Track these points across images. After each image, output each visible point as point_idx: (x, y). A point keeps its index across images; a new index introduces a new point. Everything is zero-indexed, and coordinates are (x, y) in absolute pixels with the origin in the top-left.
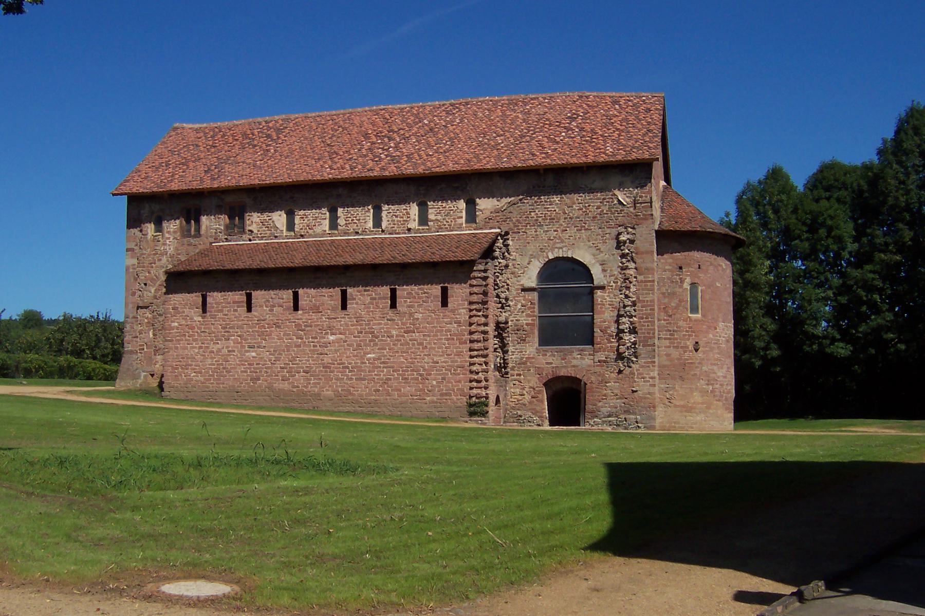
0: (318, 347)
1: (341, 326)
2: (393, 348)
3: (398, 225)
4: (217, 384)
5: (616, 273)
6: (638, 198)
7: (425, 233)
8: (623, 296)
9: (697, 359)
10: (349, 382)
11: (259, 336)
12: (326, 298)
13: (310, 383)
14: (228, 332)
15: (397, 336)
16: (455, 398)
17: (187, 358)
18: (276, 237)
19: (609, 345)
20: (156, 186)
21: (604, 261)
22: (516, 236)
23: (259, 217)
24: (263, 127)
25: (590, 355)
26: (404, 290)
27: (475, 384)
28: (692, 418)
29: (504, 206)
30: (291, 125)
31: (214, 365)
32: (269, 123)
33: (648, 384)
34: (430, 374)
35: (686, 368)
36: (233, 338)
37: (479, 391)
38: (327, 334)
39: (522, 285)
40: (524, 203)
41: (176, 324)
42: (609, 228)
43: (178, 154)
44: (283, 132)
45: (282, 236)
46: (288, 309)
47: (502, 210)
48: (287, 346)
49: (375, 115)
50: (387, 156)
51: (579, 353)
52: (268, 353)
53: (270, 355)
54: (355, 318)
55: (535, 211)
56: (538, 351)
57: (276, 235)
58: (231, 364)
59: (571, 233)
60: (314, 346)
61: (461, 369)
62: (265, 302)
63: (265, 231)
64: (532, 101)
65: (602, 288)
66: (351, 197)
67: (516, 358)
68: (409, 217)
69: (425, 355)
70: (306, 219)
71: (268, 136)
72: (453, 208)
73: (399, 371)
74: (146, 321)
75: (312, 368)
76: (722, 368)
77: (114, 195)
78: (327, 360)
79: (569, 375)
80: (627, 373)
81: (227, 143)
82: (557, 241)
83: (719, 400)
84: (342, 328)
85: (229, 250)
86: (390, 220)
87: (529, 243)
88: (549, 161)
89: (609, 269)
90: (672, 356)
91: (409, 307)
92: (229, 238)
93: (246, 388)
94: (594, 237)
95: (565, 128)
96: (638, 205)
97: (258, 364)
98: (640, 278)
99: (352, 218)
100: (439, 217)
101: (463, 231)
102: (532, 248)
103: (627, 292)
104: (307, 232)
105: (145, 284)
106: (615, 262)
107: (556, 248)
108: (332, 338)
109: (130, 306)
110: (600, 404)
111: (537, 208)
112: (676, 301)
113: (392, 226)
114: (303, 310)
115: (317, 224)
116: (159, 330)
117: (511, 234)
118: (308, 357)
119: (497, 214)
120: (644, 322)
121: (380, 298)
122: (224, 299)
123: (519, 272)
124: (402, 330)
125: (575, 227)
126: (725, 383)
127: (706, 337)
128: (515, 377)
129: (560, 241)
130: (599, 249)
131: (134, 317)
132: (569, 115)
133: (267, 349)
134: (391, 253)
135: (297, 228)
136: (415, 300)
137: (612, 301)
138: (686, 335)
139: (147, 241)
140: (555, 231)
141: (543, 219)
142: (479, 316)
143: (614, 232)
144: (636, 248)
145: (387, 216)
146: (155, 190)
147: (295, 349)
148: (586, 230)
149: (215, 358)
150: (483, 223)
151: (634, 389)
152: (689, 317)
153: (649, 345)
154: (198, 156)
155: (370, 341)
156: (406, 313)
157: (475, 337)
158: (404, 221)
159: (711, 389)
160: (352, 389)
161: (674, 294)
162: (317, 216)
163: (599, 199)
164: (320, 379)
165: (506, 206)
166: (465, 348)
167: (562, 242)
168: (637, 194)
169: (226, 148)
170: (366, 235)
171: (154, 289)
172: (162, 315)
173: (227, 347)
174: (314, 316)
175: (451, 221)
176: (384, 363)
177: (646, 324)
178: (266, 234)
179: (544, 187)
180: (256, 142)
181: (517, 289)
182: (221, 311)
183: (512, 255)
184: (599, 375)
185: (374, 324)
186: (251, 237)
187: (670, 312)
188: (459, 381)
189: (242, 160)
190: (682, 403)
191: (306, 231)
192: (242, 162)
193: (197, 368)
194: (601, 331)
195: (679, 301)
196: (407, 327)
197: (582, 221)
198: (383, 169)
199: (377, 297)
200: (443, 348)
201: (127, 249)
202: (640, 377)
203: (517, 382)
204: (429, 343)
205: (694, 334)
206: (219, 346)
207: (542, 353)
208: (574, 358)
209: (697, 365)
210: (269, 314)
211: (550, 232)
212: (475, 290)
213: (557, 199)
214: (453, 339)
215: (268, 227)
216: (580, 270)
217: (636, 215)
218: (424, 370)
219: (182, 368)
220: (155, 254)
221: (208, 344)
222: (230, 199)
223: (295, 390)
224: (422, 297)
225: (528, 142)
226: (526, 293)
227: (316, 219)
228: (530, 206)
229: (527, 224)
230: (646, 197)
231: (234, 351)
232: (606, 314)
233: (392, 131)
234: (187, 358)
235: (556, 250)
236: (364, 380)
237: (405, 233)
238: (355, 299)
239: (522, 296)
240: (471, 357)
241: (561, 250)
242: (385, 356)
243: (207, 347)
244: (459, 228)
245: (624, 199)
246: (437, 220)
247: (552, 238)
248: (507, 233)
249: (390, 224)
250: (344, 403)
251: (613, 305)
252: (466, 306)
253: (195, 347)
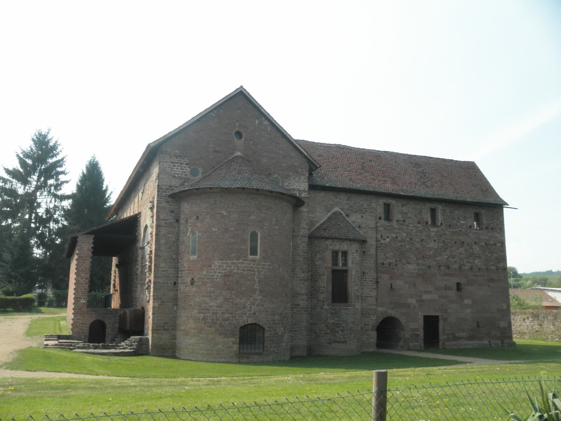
76: (216, 299)
83: (211, 327)
90: (181, 290)
112: (184, 247)
126: (220, 312)
159: (202, 316)
209: (192, 297)
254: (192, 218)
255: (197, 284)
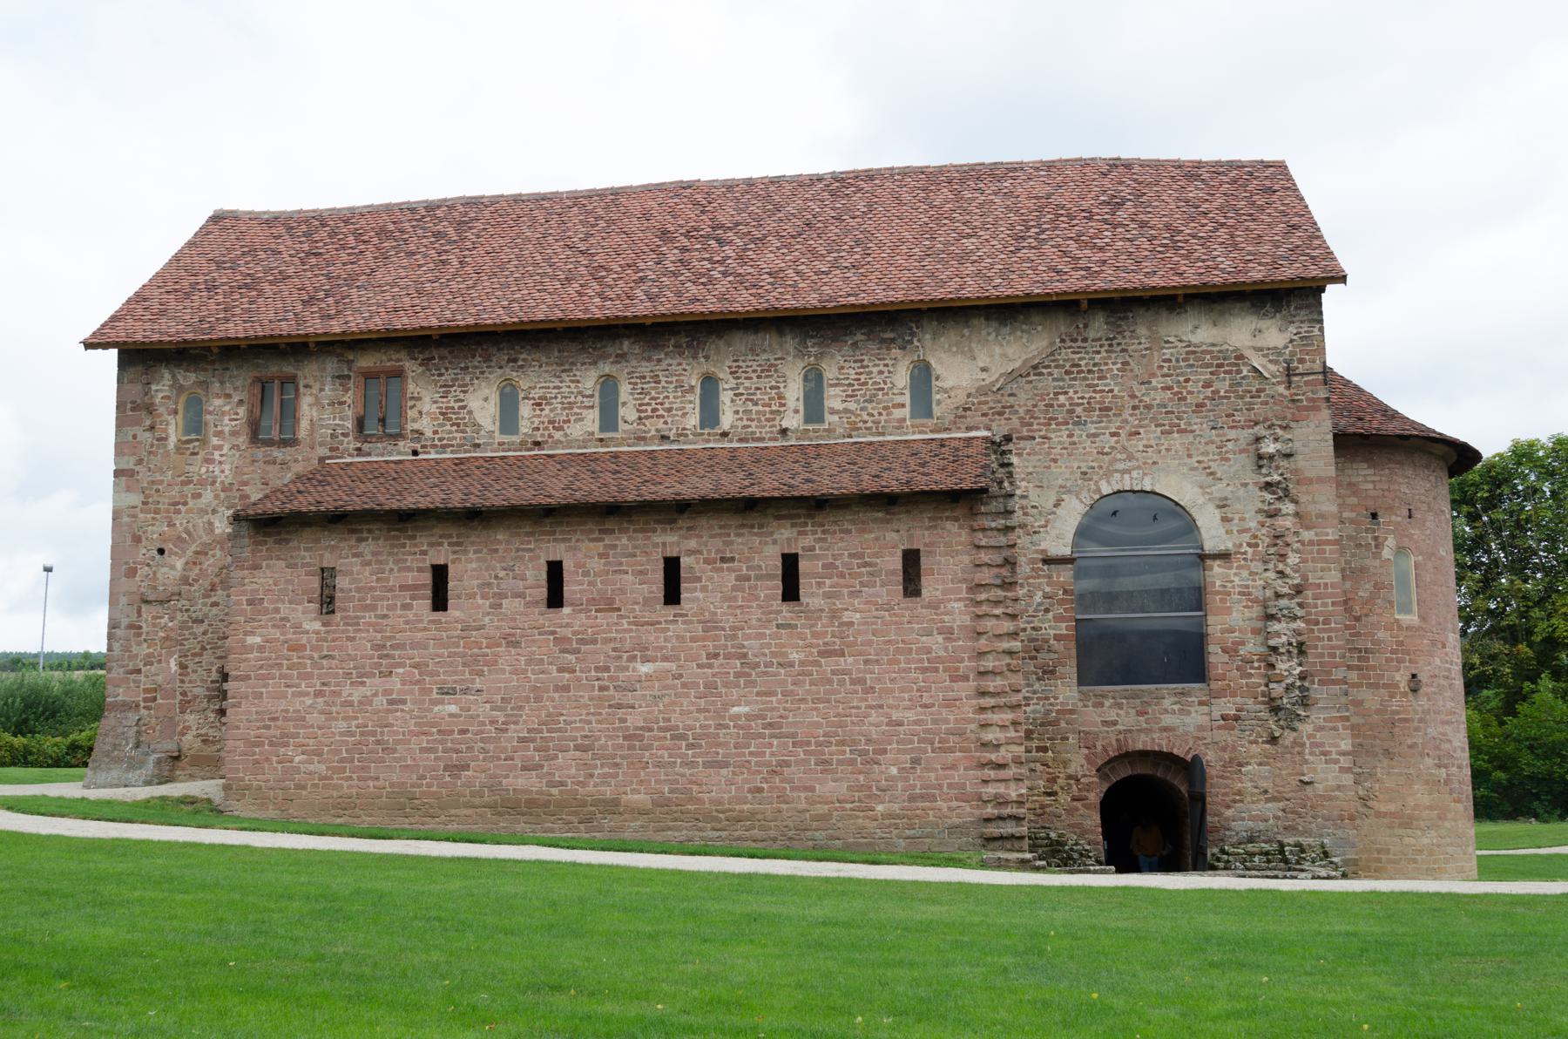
0: (612, 692)
1: (666, 640)
2: (792, 691)
3: (759, 420)
4: (359, 779)
5: (1253, 524)
6: (1296, 364)
7: (822, 438)
8: (1271, 575)
9: (1415, 711)
10: (688, 772)
11: (464, 665)
12: (630, 577)
13: (592, 776)
14: (387, 656)
15: (802, 663)
16: (944, 805)
17: (286, 719)
18: (478, 446)
19: (1244, 681)
20: (190, 329)
21: (1226, 499)
22: (1027, 444)
23: (435, 402)
24: (423, 217)
25: (1201, 703)
26: (817, 557)
27: (992, 774)
28: (1413, 841)
29: (997, 380)
30: (487, 213)
31: (352, 734)
32: (433, 210)
33: (1337, 766)
34: (884, 751)
35: (1397, 731)
36: (401, 670)
37: (1000, 789)
38: (632, 659)
39: (1044, 551)
40: (1043, 374)
41: (258, 640)
42: (1232, 427)
43: (230, 268)
44: (470, 228)
45: (492, 444)
46: (537, 602)
47: (995, 389)
48: (534, 689)
49: (671, 198)
50: (725, 274)
51: (1177, 699)
52: (488, 705)
53: (492, 709)
54: (699, 622)
55: (1066, 393)
56: (1084, 698)
57: (477, 441)
58: (397, 733)
59: (1148, 439)
60: (602, 689)
61: (956, 739)
62: (481, 586)
63: (450, 432)
64: (1011, 174)
65: (1224, 556)
66: (649, 360)
67: (1034, 712)
68: (784, 405)
69: (870, 707)
70: (547, 408)
71: (438, 235)
72: (882, 386)
73: (808, 743)
74: (162, 634)
75: (599, 739)
77: (88, 345)
78: (634, 720)
79: (1156, 749)
80: (1287, 742)
81: (343, 247)
82: (1119, 456)
83: (1459, 801)
84: (669, 645)
85: (375, 472)
86: (741, 410)
87: (1055, 461)
88: (1100, 284)
89: (1237, 517)
90: (1367, 705)
91: (827, 596)
92: (366, 447)
93: (434, 789)
94: (1202, 448)
95: (1105, 221)
96: (1296, 379)
97: (463, 732)
98: (1307, 535)
99: (654, 406)
100: (852, 406)
101: (906, 434)
102: (1063, 472)
103: (1281, 567)
104: (550, 436)
105: (161, 551)
106: (1250, 503)
107: (1116, 471)
108: (645, 669)
109: (123, 600)
110: (1229, 813)
111: (1070, 386)
113: (745, 423)
114: (572, 605)
115: (572, 418)
116: (195, 655)
117: (1014, 440)
118: (588, 714)
119: (983, 398)
120: (1320, 631)
121: (758, 578)
122: (378, 580)
123: (1036, 524)
124: (815, 650)
125: (1156, 426)
127: (1430, 664)
128: (1034, 754)
129: (1124, 456)
130: (1212, 474)
131: (131, 626)
132: (1102, 198)
133: (485, 696)
134: (773, 476)
135: (525, 427)
136: (842, 581)
137: (1247, 587)
138: (1392, 659)
139: (167, 454)
140: (1113, 434)
141: (1084, 410)
142: (997, 616)
143: (1246, 435)
144: (1296, 471)
145: (732, 401)
146: (190, 337)
147: (556, 695)
148: (1181, 431)
149: (357, 718)
150: (952, 417)
151: (1306, 779)
152: (1397, 621)
153: (1335, 682)
154: (280, 272)
155: (737, 675)
156: (822, 610)
157: (989, 663)
158: (772, 412)
160: (695, 788)
161: (1363, 570)
162: (572, 399)
163: (1208, 366)
164: (617, 765)
165: (1002, 380)
166: (965, 689)
167: (1130, 458)
168: (1293, 354)
169: (345, 258)
170: (685, 443)
171: (183, 561)
172: (202, 621)
173: (387, 692)
174: (602, 619)
175: (880, 414)
176: (770, 725)
177: (1326, 636)
178: (455, 438)
179: (1085, 340)
180: (413, 247)
181: (1033, 561)
182: (373, 608)
183: (1019, 488)
184: (1224, 749)
185: (748, 637)
186: (419, 446)
187: (1357, 610)
188: (953, 767)
189: (389, 279)
190: (1392, 807)
191: (546, 433)
192: (388, 284)
193: (311, 742)
194: (1224, 651)
195: (1375, 585)
196: (826, 644)
197: (1173, 413)
198: (722, 298)
199: (752, 573)
200: (911, 690)
201: (115, 471)
202: (1317, 751)
203: (1039, 767)
204: (879, 680)
205: (1408, 658)
206: (366, 691)
207: (1093, 699)
208: (1166, 711)
209: (1416, 724)
210: (488, 614)
211: (1102, 437)
212: (984, 557)
213: (1114, 367)
214: (936, 670)
215: (458, 425)
216: (1177, 518)
217: (1293, 401)
218: (869, 741)
219: (271, 744)
220: (184, 483)
221: (337, 684)
222: (367, 361)
223: (555, 791)
224: (861, 575)
225: (1033, 248)
226: (1052, 566)
227: (572, 408)
228: (1054, 380)
229: (1051, 419)
230: (1314, 362)
231: (403, 702)
232: (1235, 614)
233: (721, 226)
234: (286, 719)
235: (1117, 476)
236: (727, 765)
237: (776, 439)
238: (699, 579)
239: (1044, 576)
240: (983, 709)
241: (1127, 476)
242: (773, 709)
243: (334, 693)
244: (898, 428)
245: (1264, 367)
246: (846, 411)
247: (1106, 450)
248: (1008, 439)
249: (741, 419)
250: (676, 820)
251: (1249, 594)
252: (964, 595)
253: (307, 694)
254: (1398, 512)
255: (1430, 690)
